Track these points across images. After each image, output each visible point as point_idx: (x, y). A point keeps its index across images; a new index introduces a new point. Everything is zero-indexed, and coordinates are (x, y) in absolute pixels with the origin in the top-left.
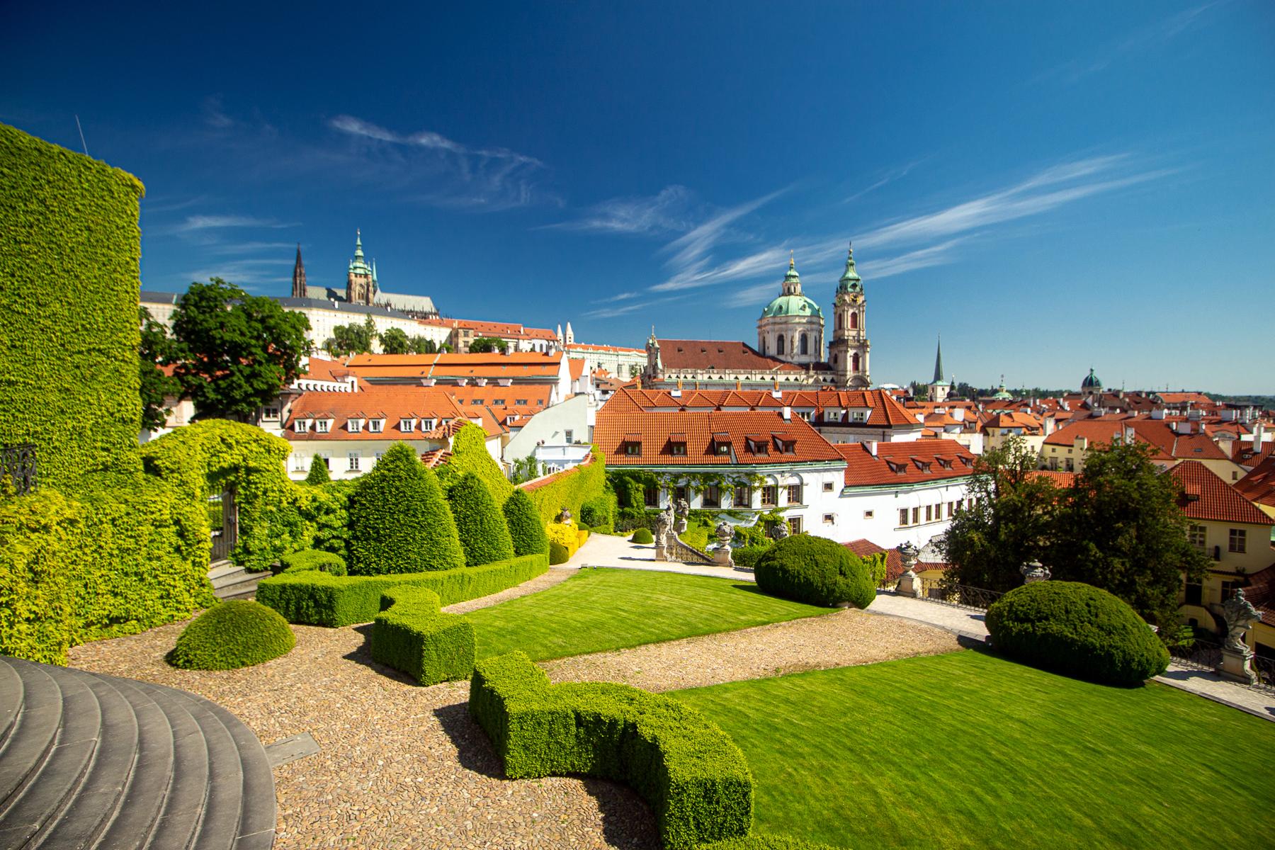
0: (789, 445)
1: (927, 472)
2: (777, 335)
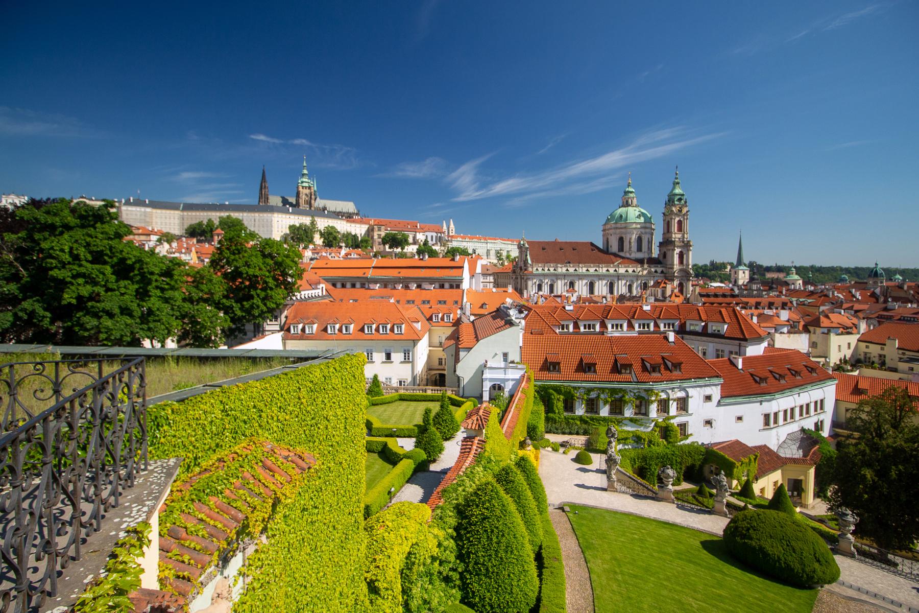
0: (677, 366)
1: (783, 382)
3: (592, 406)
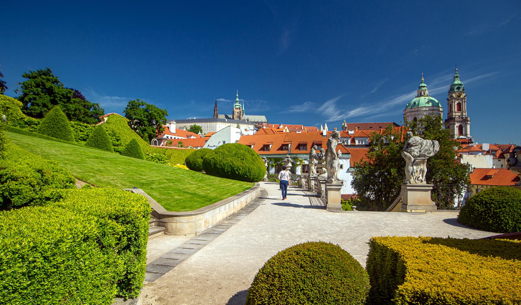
2: (413, 117)
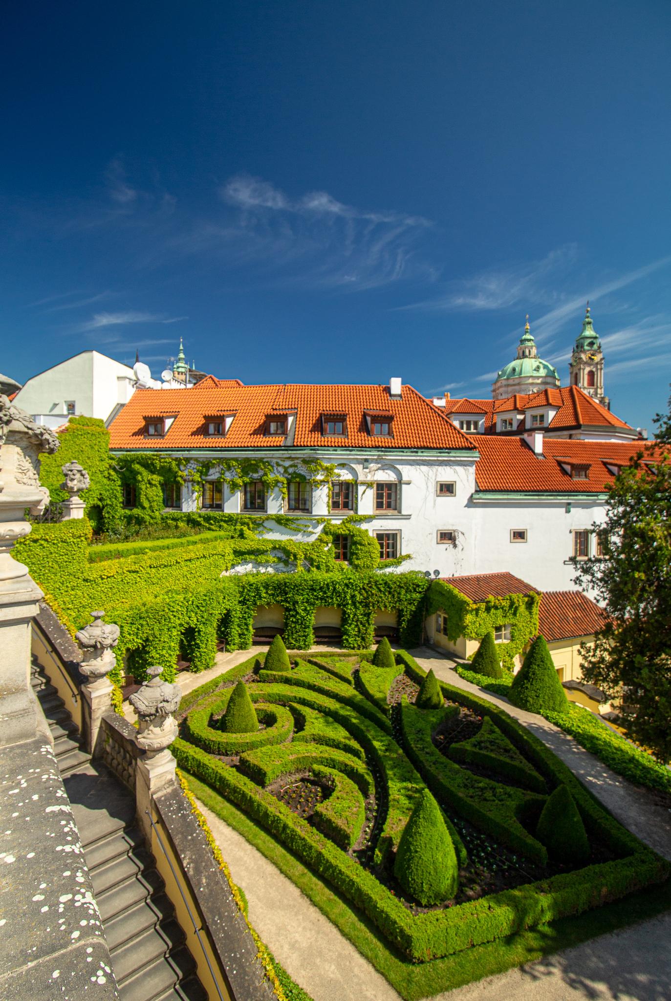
3: (215, 494)
